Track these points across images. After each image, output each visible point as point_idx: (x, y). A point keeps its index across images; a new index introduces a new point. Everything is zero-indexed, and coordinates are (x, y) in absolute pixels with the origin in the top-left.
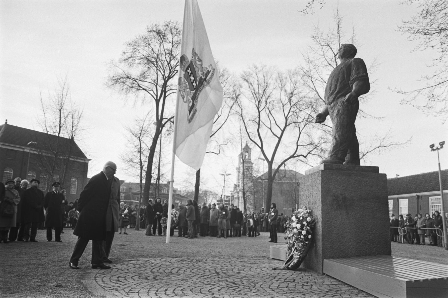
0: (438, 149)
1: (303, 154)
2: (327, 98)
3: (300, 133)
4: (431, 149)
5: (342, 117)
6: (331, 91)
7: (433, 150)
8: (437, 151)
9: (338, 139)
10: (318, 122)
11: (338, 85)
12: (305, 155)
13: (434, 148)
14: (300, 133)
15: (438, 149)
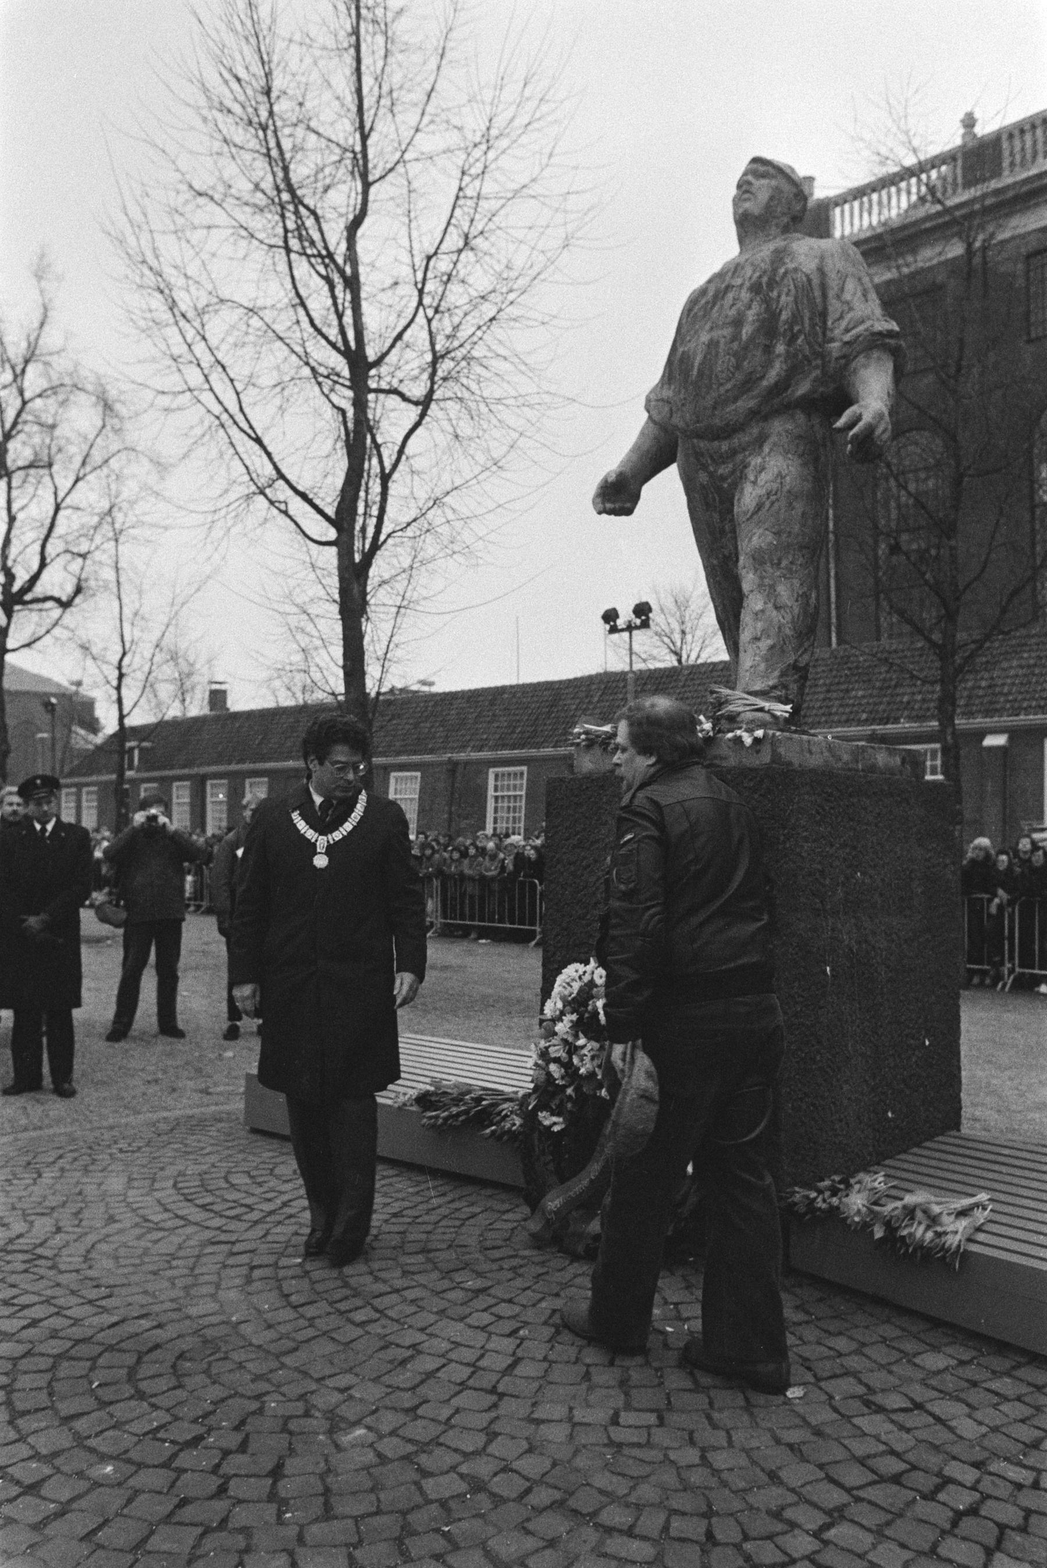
0: (630, 628)
1: (49, 593)
2: (709, 401)
3: (58, 508)
4: (608, 627)
5: (799, 507)
6: (739, 376)
7: (614, 630)
8: (626, 635)
9: (789, 617)
10: (610, 512)
11: (780, 348)
12: (64, 599)
13: (621, 623)
14: (58, 508)
15: (630, 628)
